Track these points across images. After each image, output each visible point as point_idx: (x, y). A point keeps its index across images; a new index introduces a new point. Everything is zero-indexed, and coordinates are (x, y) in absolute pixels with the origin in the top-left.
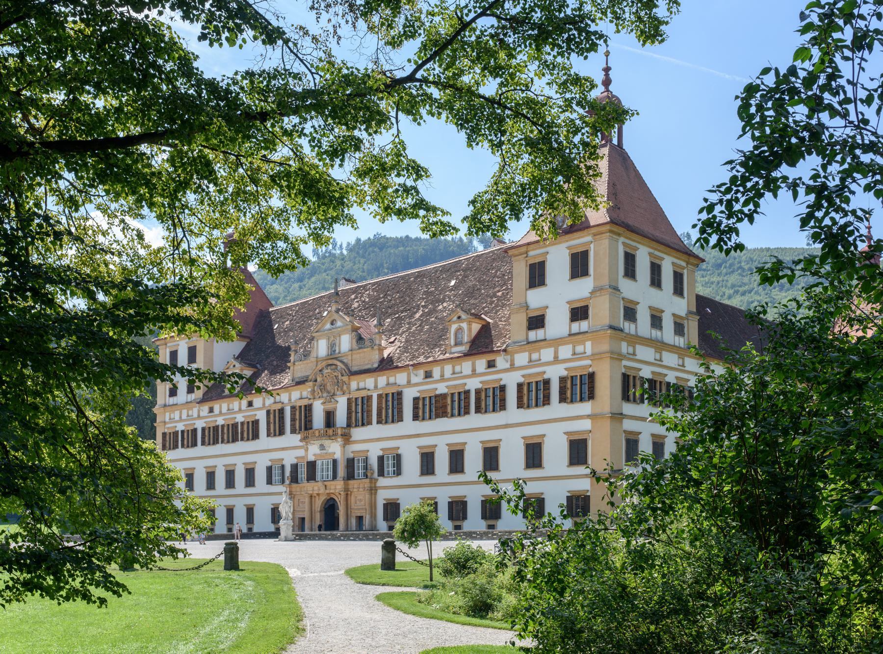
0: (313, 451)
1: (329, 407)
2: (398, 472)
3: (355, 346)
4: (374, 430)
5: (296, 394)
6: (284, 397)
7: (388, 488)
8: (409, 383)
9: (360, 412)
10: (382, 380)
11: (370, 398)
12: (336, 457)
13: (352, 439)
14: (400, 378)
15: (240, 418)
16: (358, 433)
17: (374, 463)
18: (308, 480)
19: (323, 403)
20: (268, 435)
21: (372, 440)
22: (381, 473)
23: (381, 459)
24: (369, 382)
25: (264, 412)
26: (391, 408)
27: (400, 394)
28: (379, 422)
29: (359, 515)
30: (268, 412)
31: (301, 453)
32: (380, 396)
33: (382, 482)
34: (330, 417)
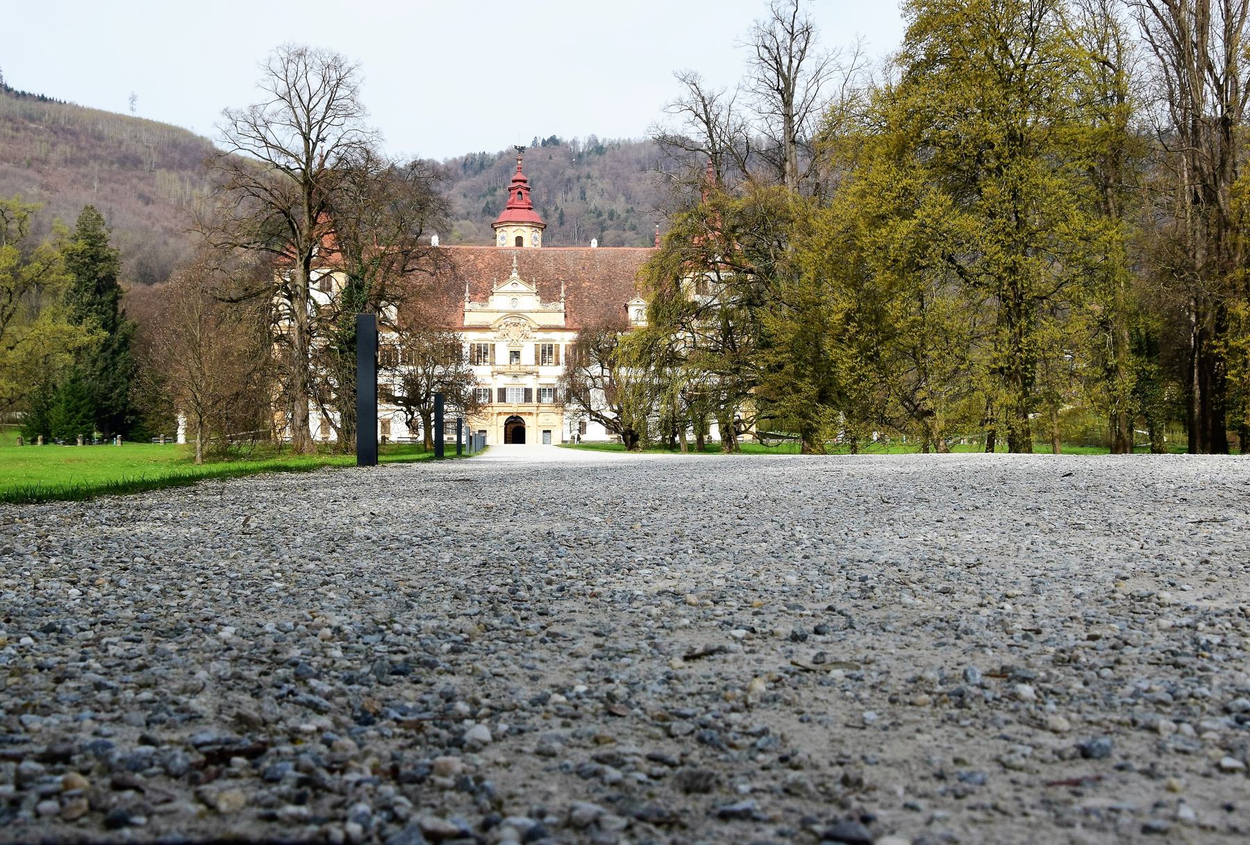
3: (538, 306)
34: (515, 355)
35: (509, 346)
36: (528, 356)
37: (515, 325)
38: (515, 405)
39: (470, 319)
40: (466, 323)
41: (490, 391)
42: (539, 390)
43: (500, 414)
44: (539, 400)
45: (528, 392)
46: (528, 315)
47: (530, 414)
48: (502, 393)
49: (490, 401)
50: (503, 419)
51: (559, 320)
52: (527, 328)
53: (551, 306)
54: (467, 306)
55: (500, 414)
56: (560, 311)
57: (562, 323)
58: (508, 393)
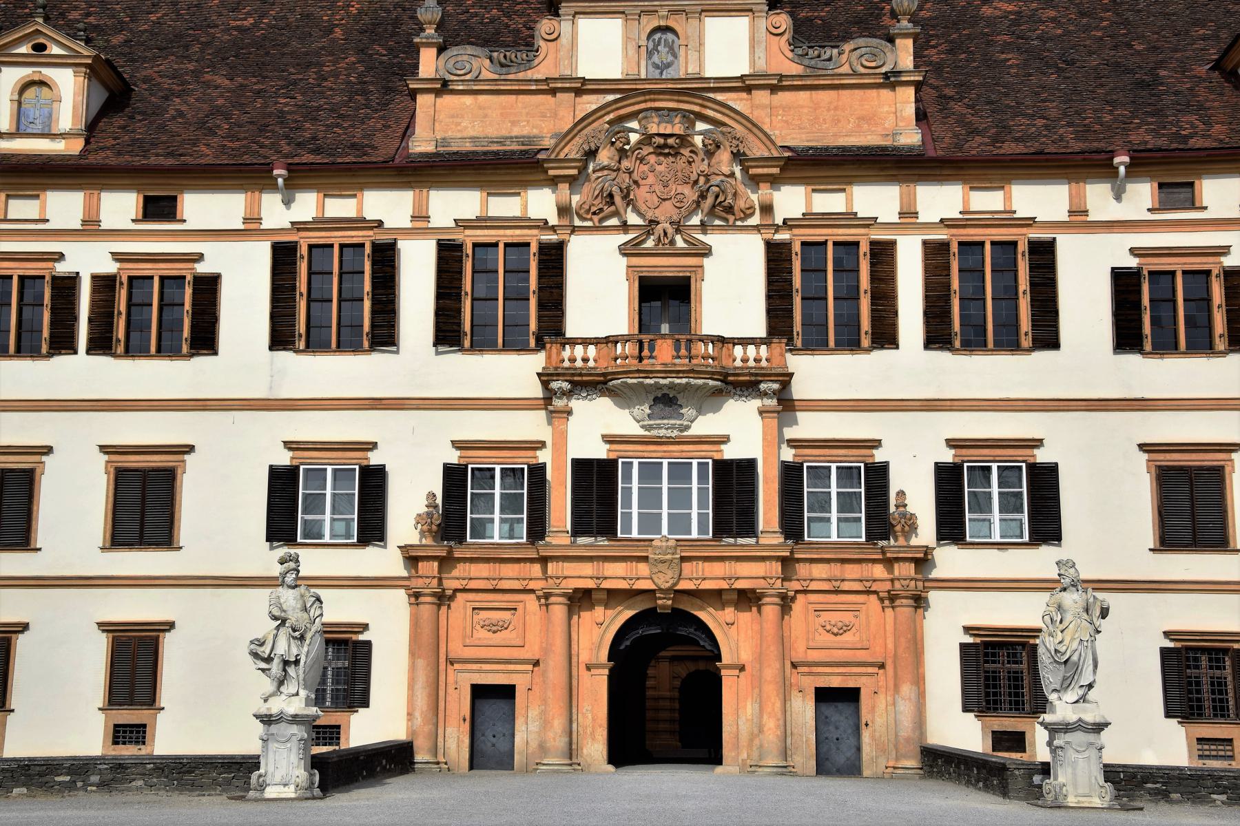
0: (594, 427)
1: (665, 266)
2: (1046, 527)
4: (910, 364)
5: (453, 206)
6: (388, 206)
7: (984, 586)
8: (1079, 220)
9: (825, 295)
10: (941, 201)
11: (883, 254)
12: (730, 452)
13: (799, 390)
14: (1039, 201)
15: (88, 261)
16: (814, 373)
17: (915, 492)
18: (580, 528)
19: (625, 250)
20: (280, 339)
21: (901, 402)
22: (951, 528)
23: (948, 480)
24: (876, 201)
25: (261, 253)
26: (994, 298)
27: (1043, 254)
28: (937, 337)
29: (836, 682)
30: (283, 256)
31: (531, 426)
32: (935, 254)
33: (951, 561)
35: (625, 250)
36: (732, 292)
37: (669, 148)
38: (664, 530)
39: (440, 122)
40: (422, 143)
41: (538, 472)
42: (791, 475)
43: (580, 599)
44: (792, 526)
45: (733, 481)
46: (737, 101)
47: (747, 599)
48: (596, 482)
49: (537, 529)
50: (598, 630)
51: (893, 118)
52: (723, 160)
53: (849, 57)
54: (429, 64)
55: (580, 599)
56: (891, 80)
57: (911, 137)
58: (631, 487)
